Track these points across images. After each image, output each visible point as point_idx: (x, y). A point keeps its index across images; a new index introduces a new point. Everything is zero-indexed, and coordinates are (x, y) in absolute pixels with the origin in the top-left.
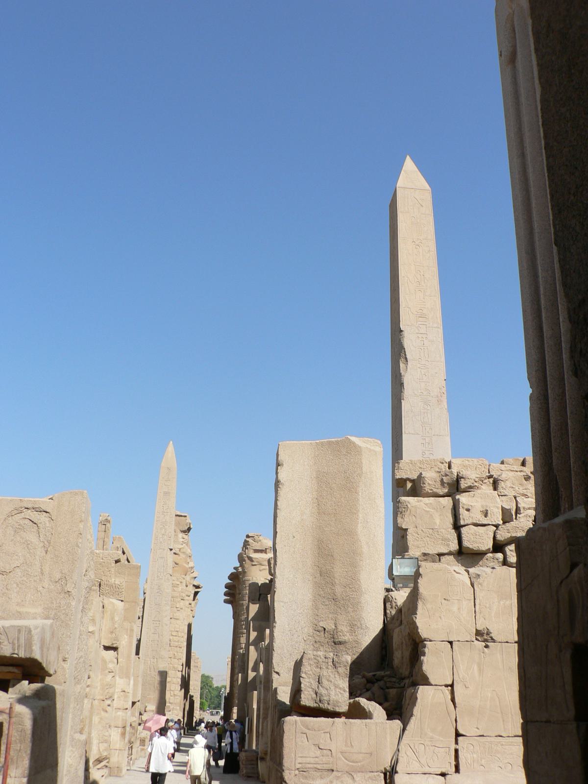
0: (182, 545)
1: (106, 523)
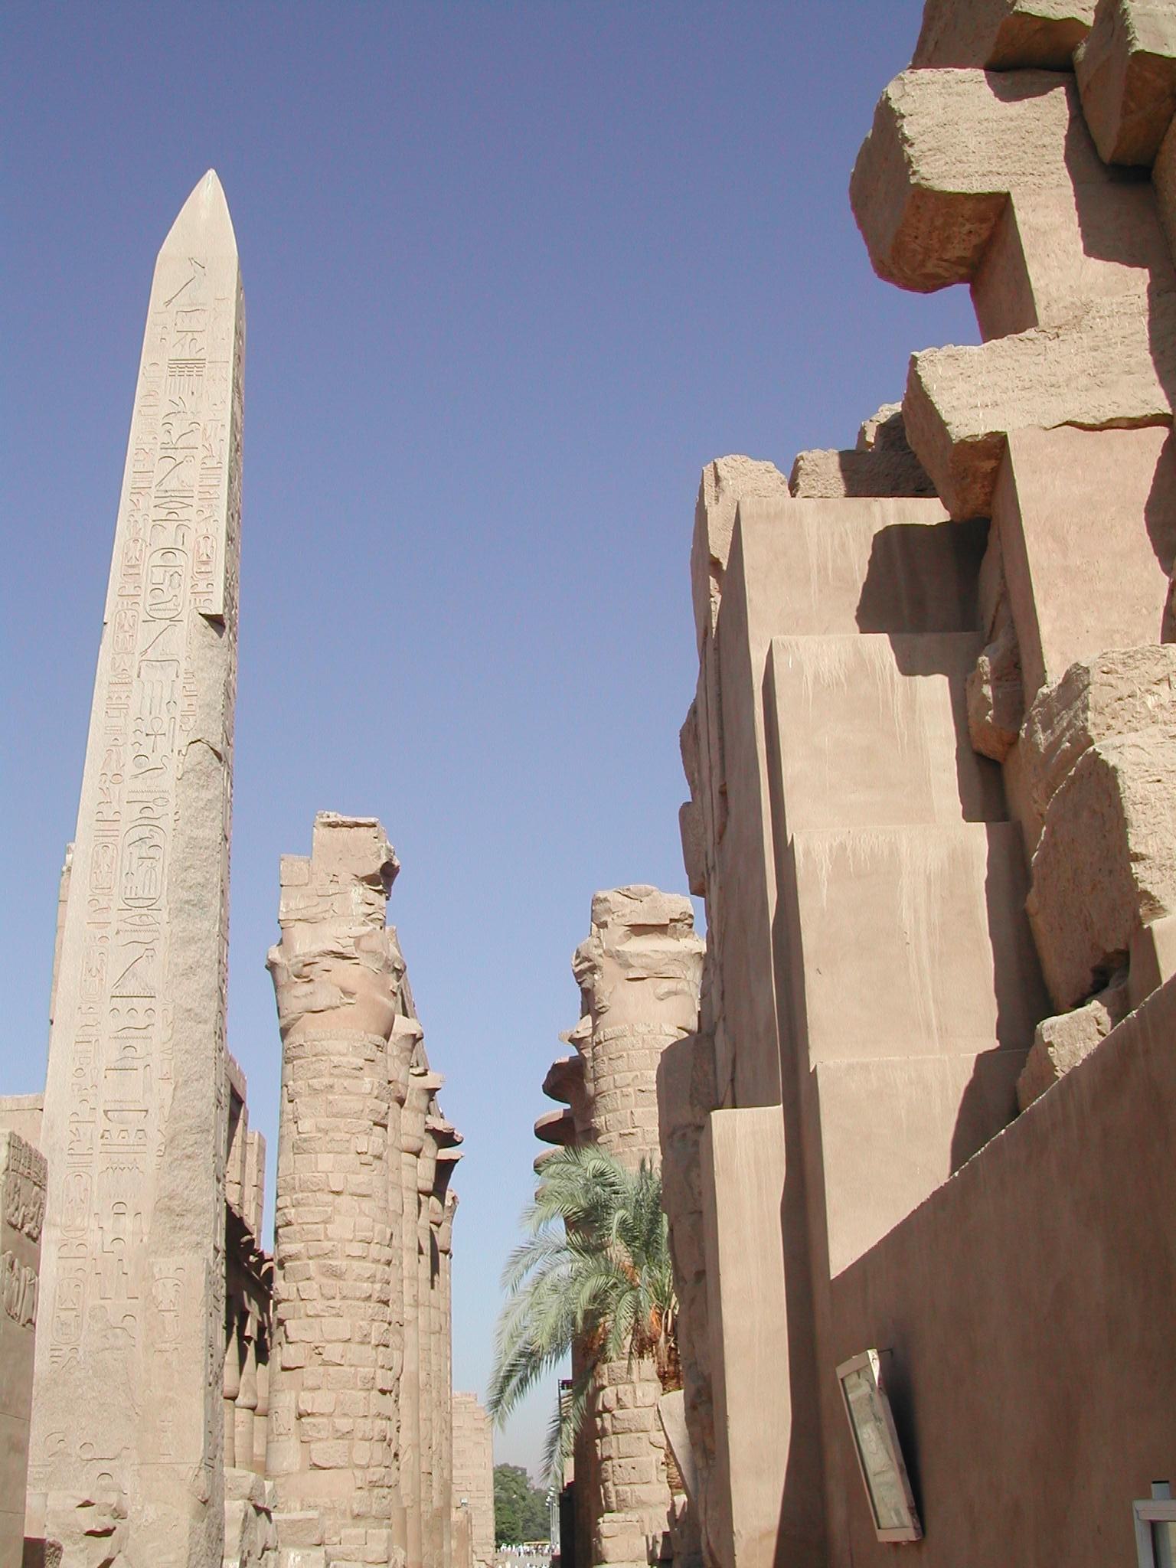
0: (364, 924)
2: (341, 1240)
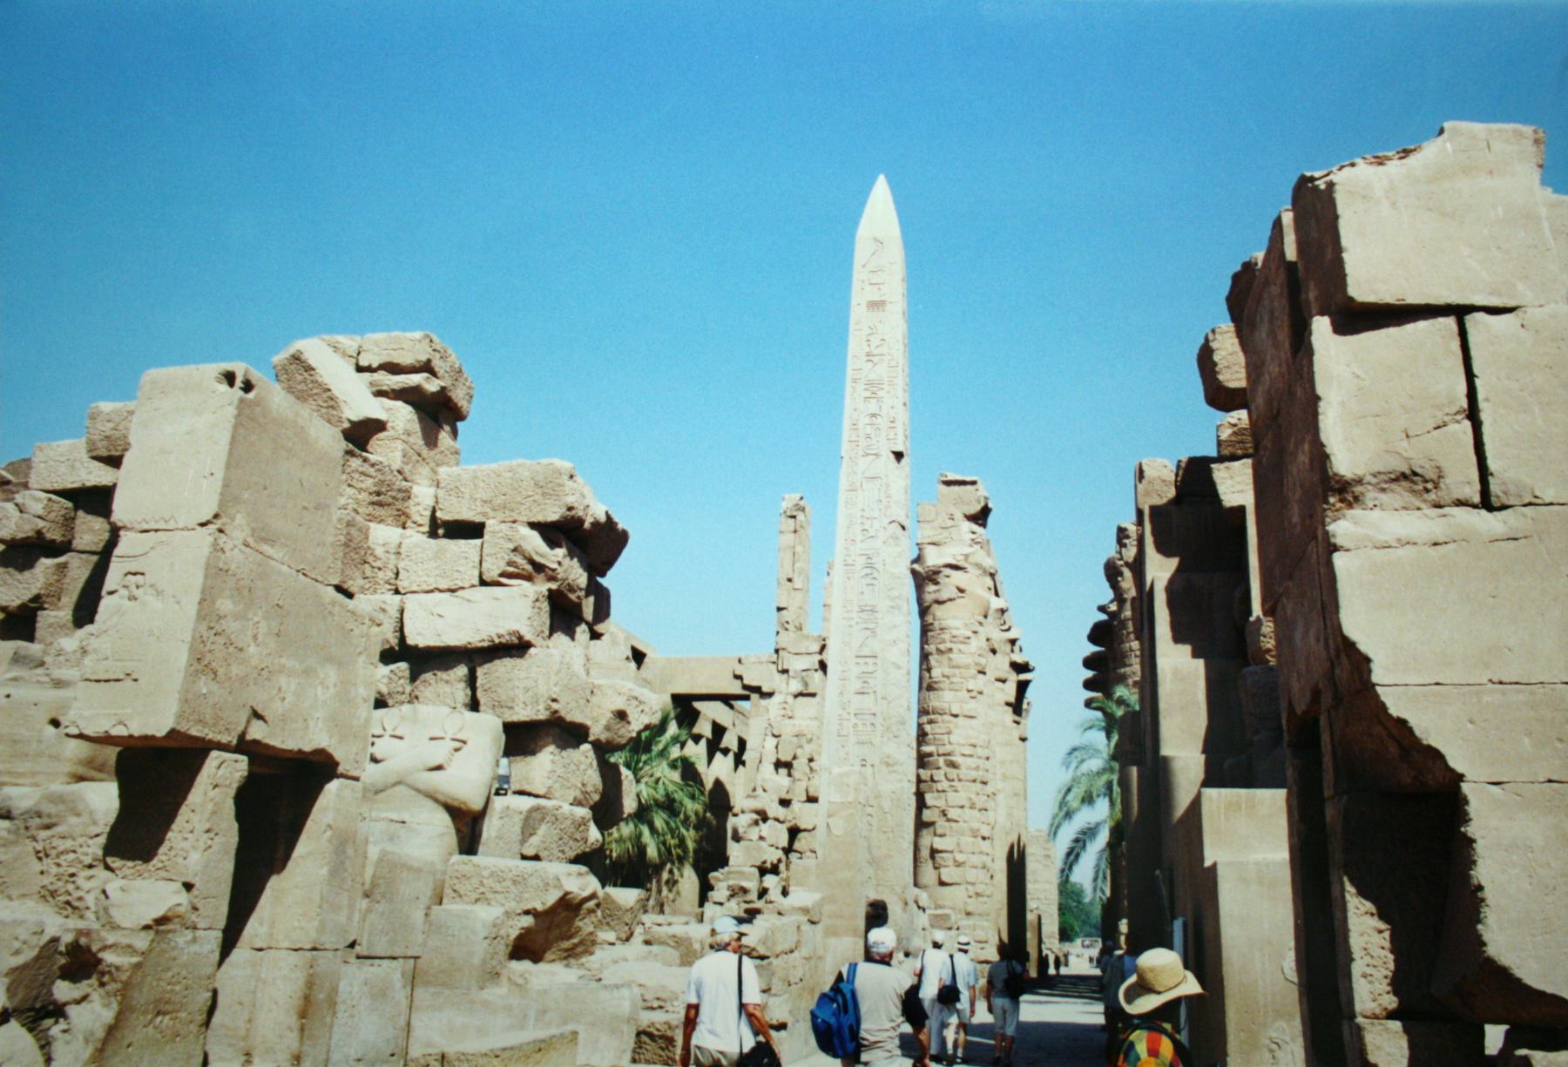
0: (971, 546)
1: (795, 513)
2: (959, 744)
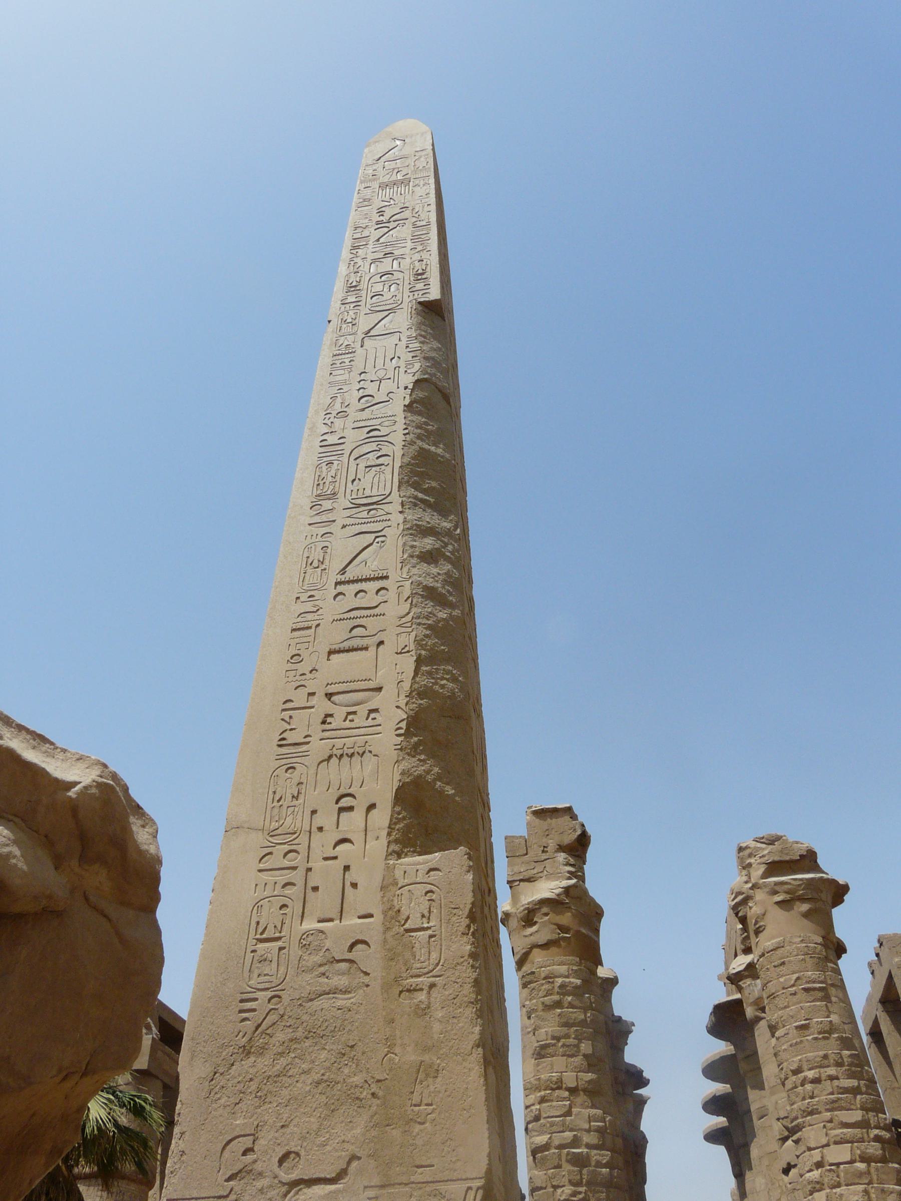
0: (569, 878)
